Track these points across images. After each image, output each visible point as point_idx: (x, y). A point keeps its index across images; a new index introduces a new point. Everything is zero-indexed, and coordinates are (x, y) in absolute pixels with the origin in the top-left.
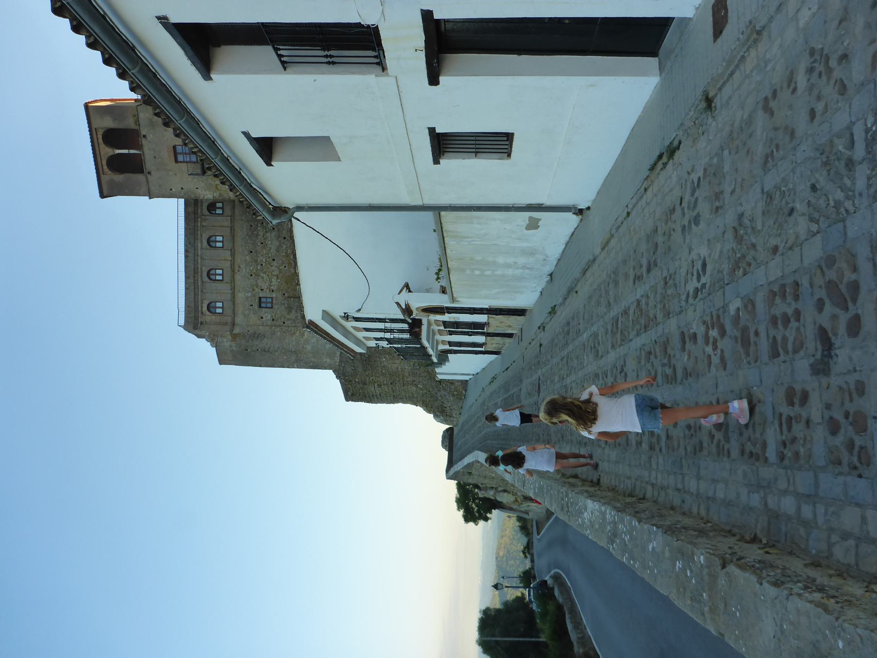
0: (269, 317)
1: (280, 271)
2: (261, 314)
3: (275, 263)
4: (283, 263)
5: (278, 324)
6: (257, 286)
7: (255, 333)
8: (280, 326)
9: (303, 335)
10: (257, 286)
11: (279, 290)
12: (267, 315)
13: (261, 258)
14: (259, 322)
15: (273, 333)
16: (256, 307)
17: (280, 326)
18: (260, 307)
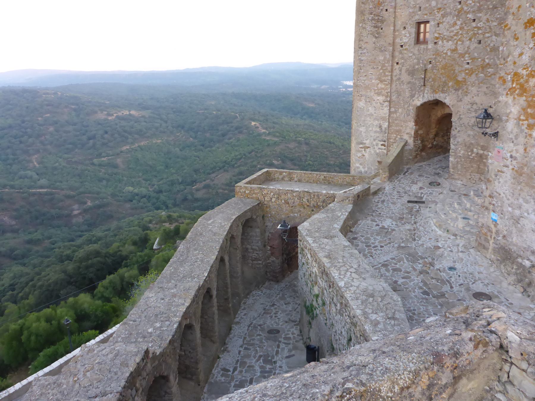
0: (405, 40)
1: (462, 55)
2: (409, 27)
3: (474, 45)
4: (473, 59)
5: (397, 54)
6: (443, 16)
7: (382, 22)
8: (393, 56)
9: (379, 94)
10: (443, 16)
11: (437, 53)
12: (407, 37)
13: (484, 18)
14: (399, 23)
15: (382, 50)
16: (417, 18)
17: (393, 56)
18: (419, 24)
